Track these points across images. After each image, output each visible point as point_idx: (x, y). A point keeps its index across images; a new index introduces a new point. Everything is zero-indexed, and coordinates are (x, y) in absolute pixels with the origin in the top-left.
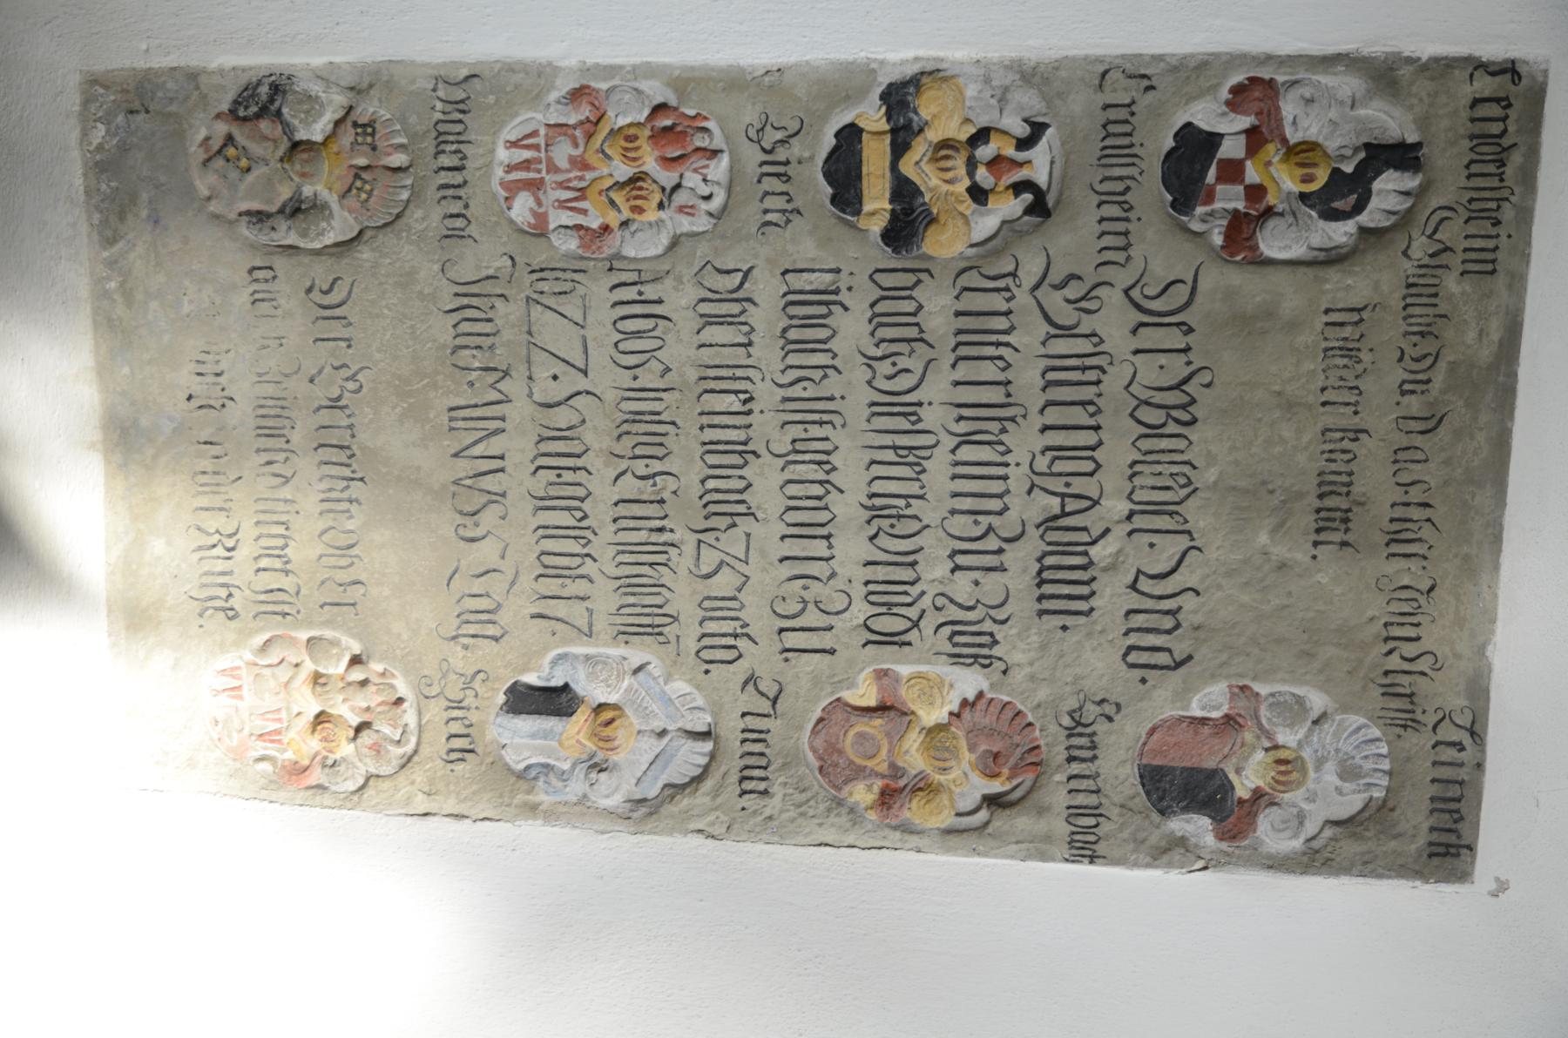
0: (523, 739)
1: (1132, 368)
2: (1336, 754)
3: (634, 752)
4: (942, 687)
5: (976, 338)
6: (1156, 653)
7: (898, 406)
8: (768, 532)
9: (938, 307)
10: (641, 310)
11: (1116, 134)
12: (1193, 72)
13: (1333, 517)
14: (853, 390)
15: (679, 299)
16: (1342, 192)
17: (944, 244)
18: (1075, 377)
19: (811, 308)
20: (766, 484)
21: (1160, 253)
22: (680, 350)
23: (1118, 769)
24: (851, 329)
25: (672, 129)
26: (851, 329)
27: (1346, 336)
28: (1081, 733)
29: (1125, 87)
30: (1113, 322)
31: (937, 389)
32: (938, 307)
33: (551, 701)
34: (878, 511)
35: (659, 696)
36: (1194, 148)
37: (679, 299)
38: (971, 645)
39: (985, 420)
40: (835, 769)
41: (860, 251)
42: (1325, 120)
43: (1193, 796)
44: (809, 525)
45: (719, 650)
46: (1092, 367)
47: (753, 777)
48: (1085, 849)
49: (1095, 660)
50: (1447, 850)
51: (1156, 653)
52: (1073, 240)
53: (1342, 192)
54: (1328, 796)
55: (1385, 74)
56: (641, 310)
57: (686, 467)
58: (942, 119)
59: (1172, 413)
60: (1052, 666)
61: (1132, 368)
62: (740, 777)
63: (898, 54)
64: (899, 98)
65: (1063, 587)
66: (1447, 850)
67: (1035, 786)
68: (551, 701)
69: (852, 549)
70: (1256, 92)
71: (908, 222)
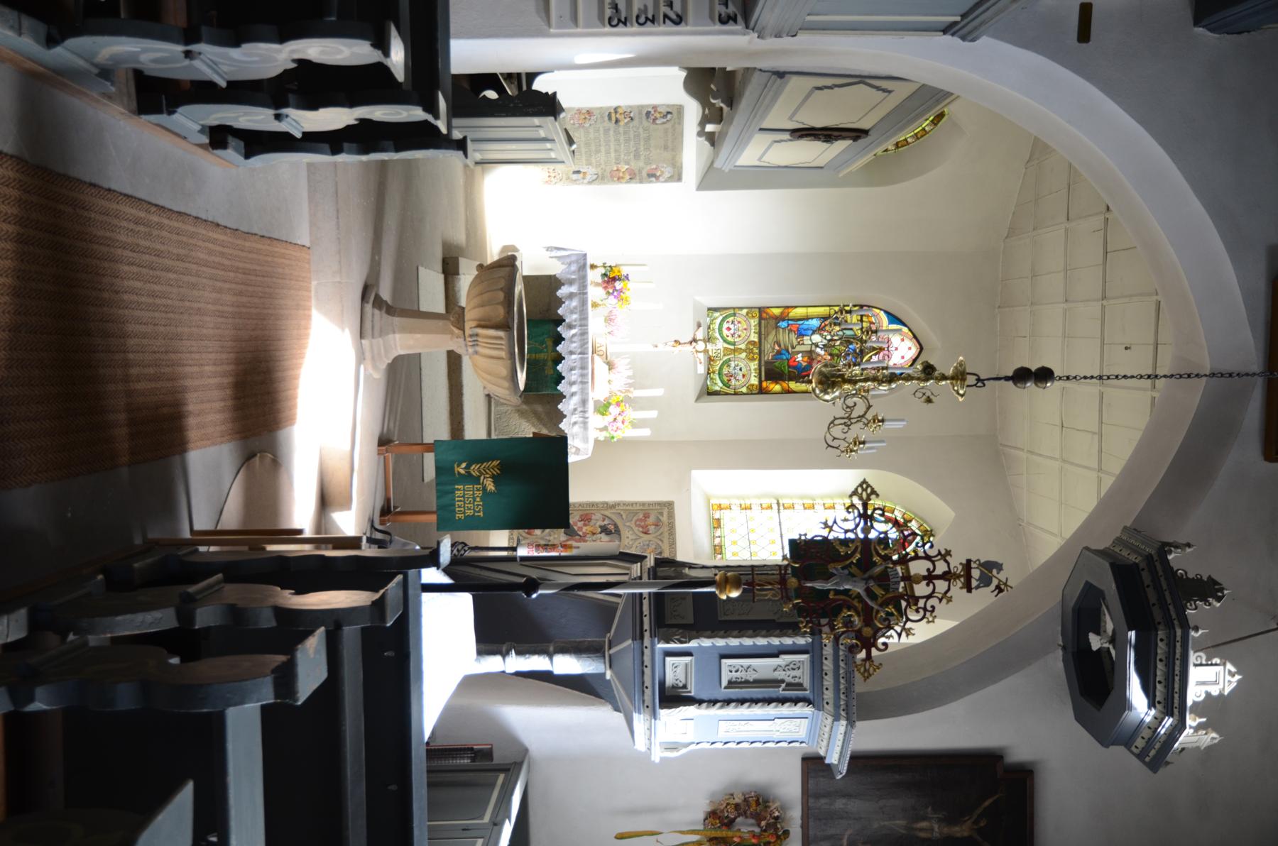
0: (575, 177)
1: (643, 135)
2: (668, 171)
3: (588, 177)
4: (624, 167)
5: (625, 133)
6: (648, 162)
7: (617, 140)
8: (603, 154)
9: (621, 130)
10: (587, 132)
11: (640, 113)
12: (648, 106)
13: (666, 148)
14: (612, 139)
15: (591, 130)
16: (665, 116)
17: (622, 123)
18: (637, 136)
19: (607, 131)
20: (603, 149)
21: (645, 123)
22: (592, 136)
23: (644, 174)
24: (612, 133)
25: (589, 112)
26: (612, 133)
27: (666, 131)
28: (640, 171)
29: (641, 107)
30: (641, 130)
31: (622, 138)
32: (621, 130)
33: (578, 172)
34: (616, 151)
35: (591, 171)
36: (648, 113)
37: (591, 130)
38: (628, 163)
39: (627, 141)
40: (612, 177)
41: (612, 125)
42: (663, 110)
43: (652, 176)
44: (608, 152)
45: (597, 167)
46: (638, 135)
47: (603, 179)
48: (641, 182)
49: (641, 164)
50: (679, 179)
51: (648, 162)
52: (635, 122)
53: (665, 116)
54: (667, 175)
55: (668, 106)
56: (587, 132)
57: (593, 148)
58: (620, 111)
59: (648, 139)
60: (635, 165)
61: (643, 135)
62: (600, 179)
63: (615, 104)
64: (616, 110)
65: (637, 156)
66: (679, 179)
67: (633, 177)
68: (578, 172)
69: (613, 155)
70: (655, 107)
71: (617, 121)
